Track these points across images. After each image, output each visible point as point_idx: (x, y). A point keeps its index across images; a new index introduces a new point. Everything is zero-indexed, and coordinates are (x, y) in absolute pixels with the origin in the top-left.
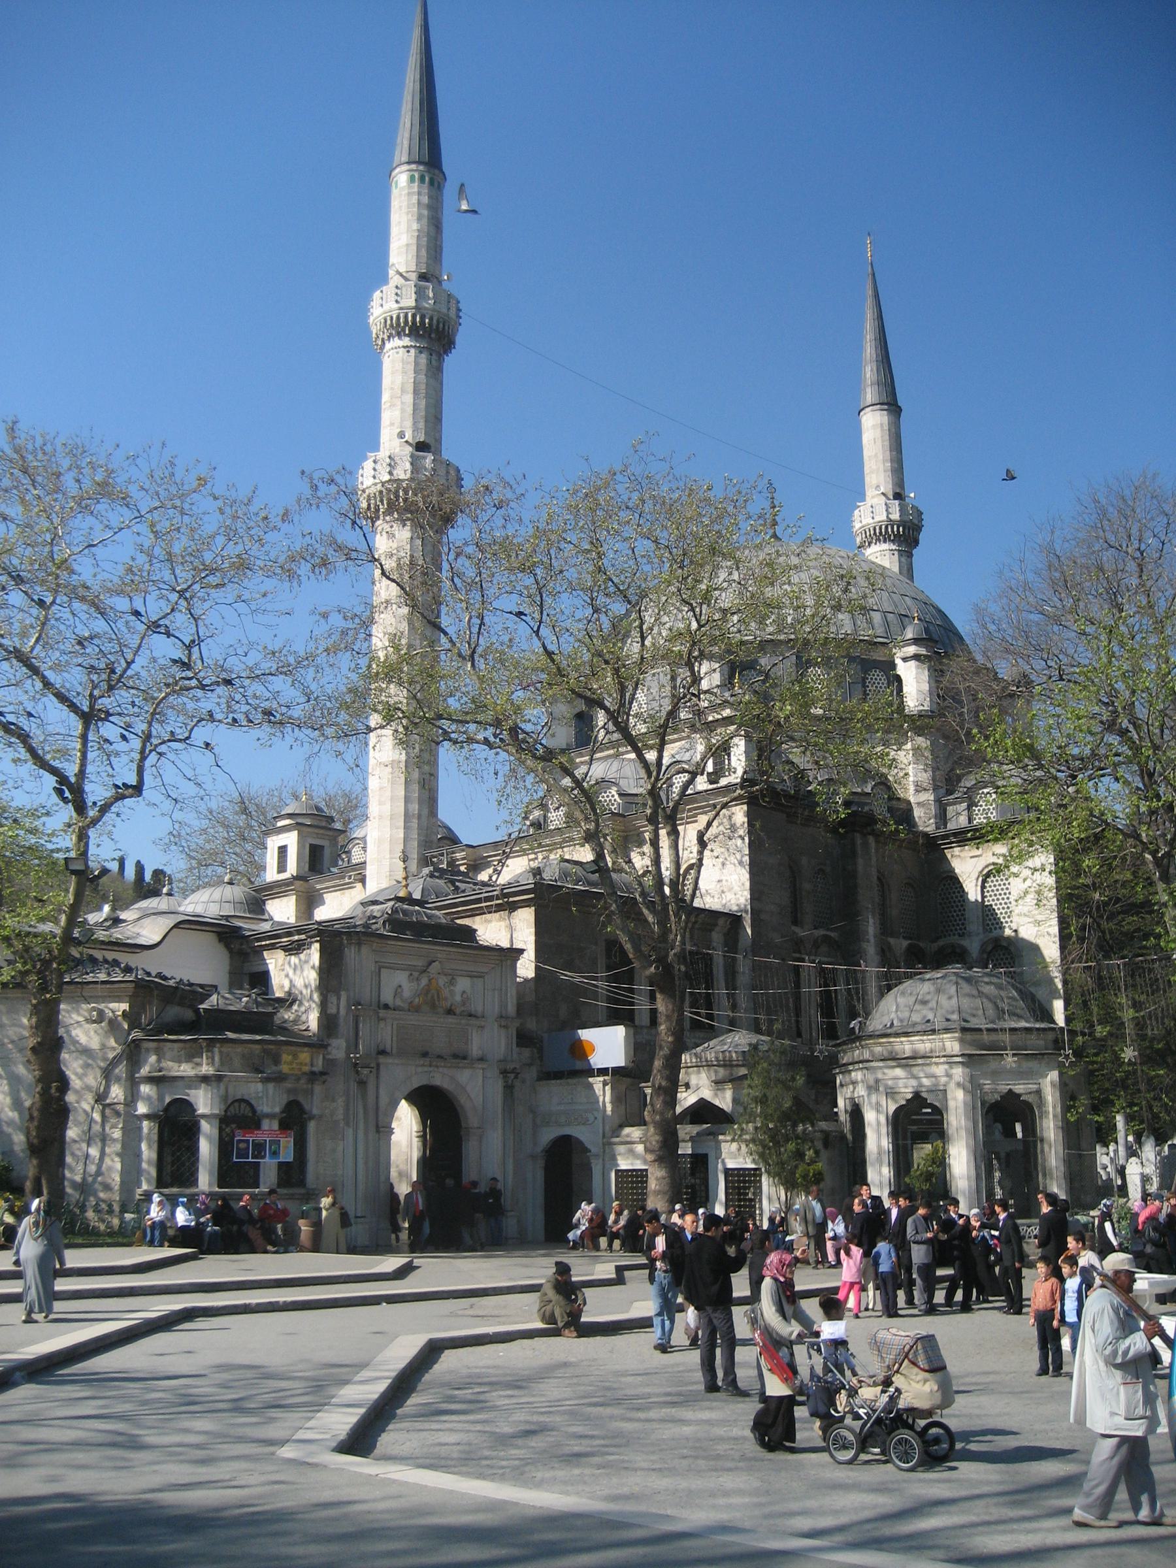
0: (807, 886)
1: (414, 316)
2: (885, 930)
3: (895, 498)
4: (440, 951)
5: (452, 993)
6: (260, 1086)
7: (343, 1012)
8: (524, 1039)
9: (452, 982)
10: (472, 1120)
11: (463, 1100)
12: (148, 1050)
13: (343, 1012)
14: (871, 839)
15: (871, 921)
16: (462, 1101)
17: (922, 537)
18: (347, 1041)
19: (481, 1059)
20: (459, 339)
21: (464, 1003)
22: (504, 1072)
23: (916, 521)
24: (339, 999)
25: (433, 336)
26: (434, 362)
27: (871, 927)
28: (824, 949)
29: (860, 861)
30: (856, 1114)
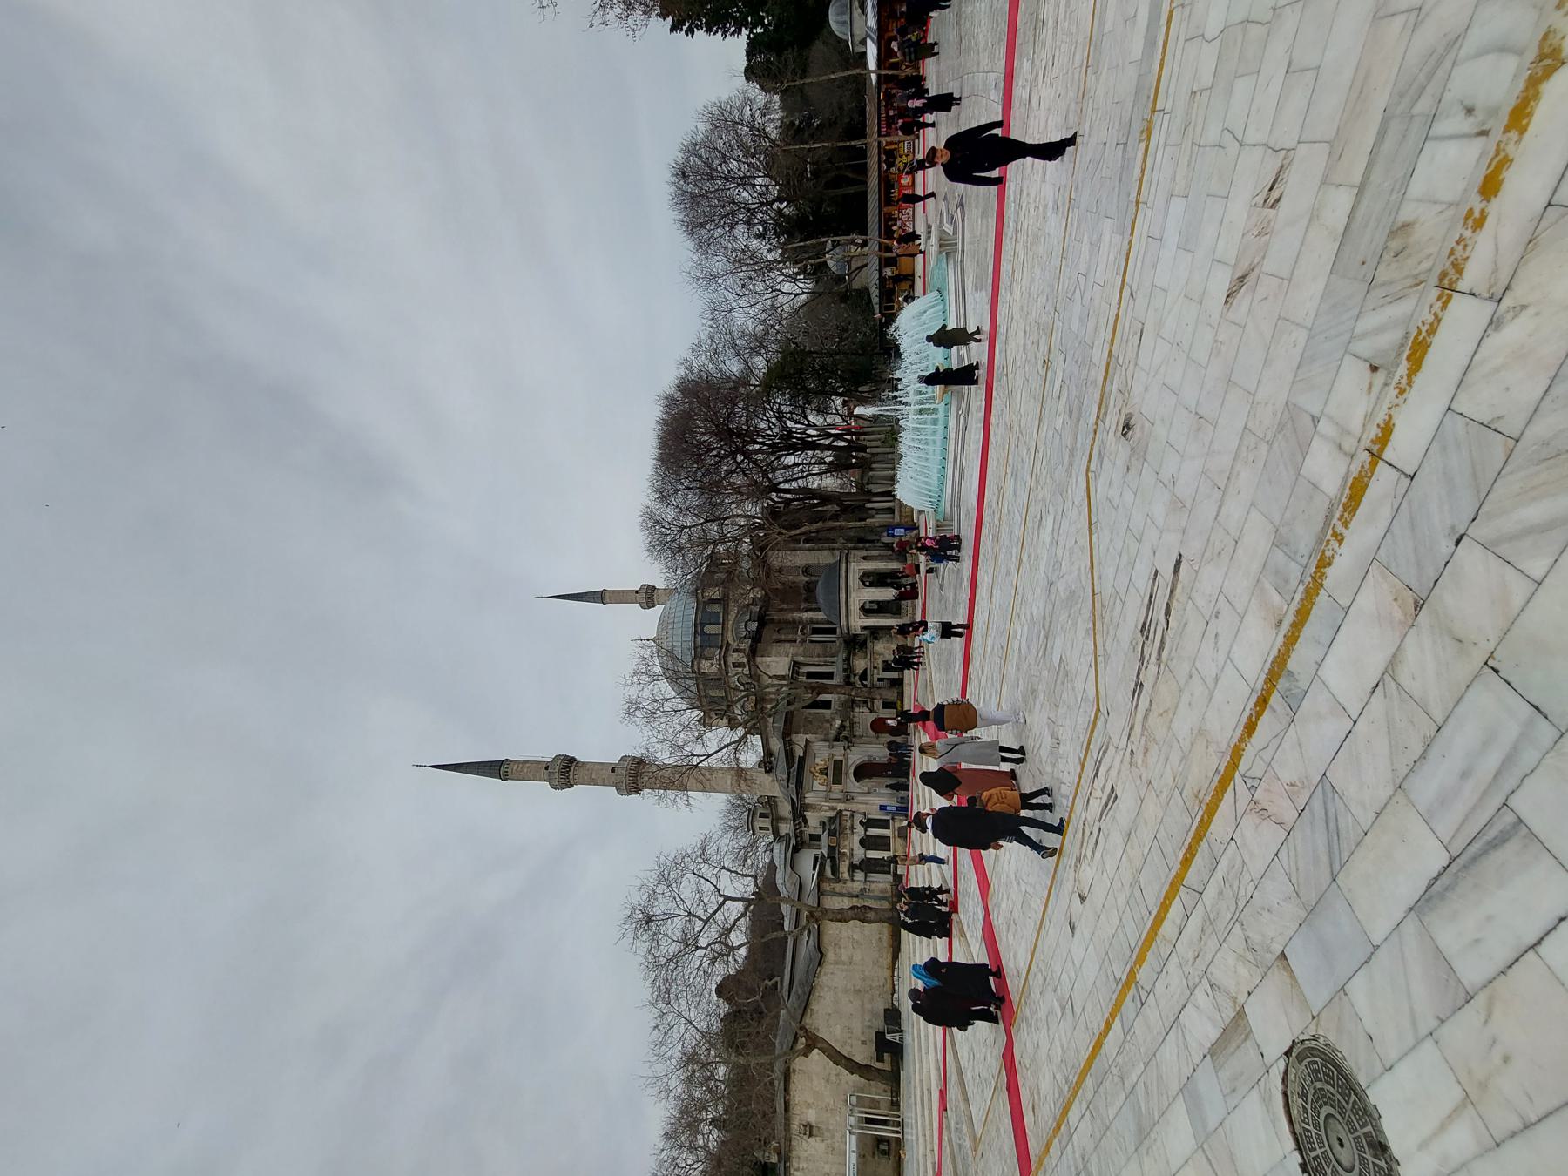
0: (783, 637)
2: (798, 610)
4: (807, 768)
11: (858, 762)
14: (768, 613)
27: (796, 615)
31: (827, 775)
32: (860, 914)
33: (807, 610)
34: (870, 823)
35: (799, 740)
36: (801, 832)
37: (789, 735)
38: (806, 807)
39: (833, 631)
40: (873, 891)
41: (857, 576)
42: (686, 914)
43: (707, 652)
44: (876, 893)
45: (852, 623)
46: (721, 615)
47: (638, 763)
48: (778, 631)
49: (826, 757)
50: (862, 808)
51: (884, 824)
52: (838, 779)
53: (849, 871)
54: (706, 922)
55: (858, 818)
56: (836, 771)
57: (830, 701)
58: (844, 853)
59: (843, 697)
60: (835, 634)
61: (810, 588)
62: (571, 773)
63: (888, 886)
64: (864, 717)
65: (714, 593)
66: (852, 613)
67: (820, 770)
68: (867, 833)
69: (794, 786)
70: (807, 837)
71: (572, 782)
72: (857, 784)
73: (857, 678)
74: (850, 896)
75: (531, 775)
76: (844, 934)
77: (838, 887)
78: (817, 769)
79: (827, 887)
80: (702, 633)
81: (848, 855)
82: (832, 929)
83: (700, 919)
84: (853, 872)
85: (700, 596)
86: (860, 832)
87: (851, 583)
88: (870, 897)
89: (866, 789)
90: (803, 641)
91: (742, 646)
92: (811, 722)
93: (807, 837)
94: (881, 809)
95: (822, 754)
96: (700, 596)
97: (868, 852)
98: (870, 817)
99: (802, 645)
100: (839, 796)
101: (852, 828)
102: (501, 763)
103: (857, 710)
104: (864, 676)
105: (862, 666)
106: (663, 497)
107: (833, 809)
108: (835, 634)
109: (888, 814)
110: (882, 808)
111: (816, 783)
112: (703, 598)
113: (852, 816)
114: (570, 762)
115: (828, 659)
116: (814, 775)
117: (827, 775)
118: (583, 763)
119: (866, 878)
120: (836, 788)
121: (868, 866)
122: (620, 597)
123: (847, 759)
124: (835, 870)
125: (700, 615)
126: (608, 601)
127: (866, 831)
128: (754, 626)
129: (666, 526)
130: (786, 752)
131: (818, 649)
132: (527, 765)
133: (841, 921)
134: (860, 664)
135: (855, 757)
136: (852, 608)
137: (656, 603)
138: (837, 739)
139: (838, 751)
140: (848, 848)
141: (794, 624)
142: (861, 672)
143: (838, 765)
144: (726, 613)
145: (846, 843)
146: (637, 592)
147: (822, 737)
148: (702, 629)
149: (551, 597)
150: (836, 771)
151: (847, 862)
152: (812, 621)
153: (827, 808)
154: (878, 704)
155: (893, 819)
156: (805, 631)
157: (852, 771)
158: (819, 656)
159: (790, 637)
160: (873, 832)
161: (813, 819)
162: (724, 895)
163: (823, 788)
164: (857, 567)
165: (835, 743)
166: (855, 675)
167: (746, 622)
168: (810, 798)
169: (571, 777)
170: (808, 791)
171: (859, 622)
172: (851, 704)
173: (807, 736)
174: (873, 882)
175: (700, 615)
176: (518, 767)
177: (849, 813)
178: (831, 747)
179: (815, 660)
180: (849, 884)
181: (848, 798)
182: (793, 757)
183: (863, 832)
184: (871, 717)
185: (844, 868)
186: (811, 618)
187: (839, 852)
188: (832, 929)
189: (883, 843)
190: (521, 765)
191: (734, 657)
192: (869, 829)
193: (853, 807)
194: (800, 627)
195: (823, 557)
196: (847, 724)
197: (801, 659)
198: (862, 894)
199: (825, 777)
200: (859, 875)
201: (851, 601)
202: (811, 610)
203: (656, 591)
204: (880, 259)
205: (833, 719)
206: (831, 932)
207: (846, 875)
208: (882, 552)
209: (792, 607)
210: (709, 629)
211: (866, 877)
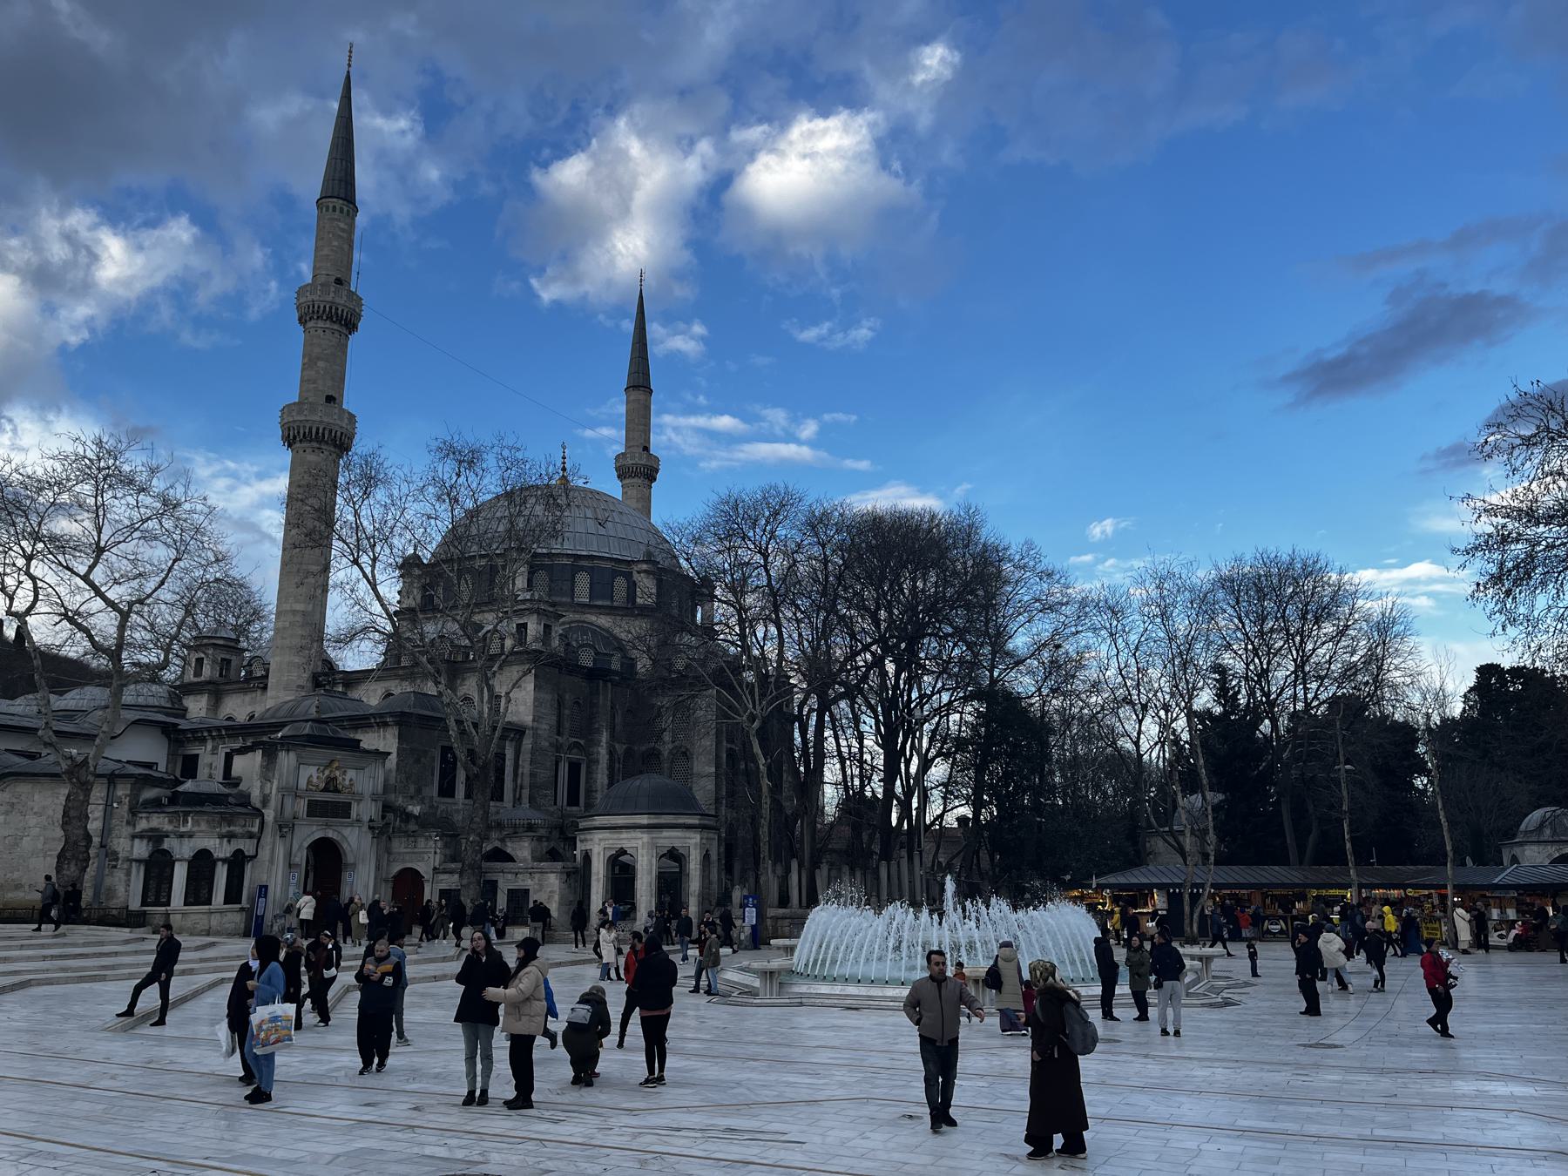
0: (567, 712)
1: (331, 308)
4: (339, 755)
5: (344, 779)
6: (218, 840)
7: (274, 792)
9: (344, 773)
11: (345, 846)
13: (274, 792)
14: (609, 685)
18: (275, 811)
24: (272, 784)
27: (604, 737)
29: (601, 697)
30: (587, 858)
31: (325, 790)
32: (75, 849)
33: (611, 753)
34: (238, 863)
35: (384, 740)
36: (203, 741)
37: (398, 723)
38: (270, 752)
39: (573, 799)
40: (111, 874)
41: (677, 844)
42: (102, 544)
43: (542, 576)
44: (108, 881)
45: (598, 835)
46: (608, 603)
48: (577, 703)
49: (358, 788)
50: (265, 854)
51: (233, 895)
52: (316, 809)
53: (152, 830)
54: (85, 578)
55: (247, 846)
56: (330, 807)
57: (453, 796)
59: (458, 818)
60: (569, 805)
61: (651, 760)
62: (328, 324)
63: (116, 903)
64: (426, 857)
65: (647, 588)
66: (616, 836)
67: (336, 778)
68: (220, 863)
69: (306, 731)
70: (194, 750)
71: (310, 324)
72: (306, 845)
73: (497, 844)
74: (106, 831)
75: (326, 251)
76: (32, 820)
77: (124, 811)
78: (337, 773)
79: (122, 791)
80: (576, 569)
81: (182, 829)
82: (49, 801)
83: (91, 568)
84: (150, 839)
85: (645, 567)
86: (222, 850)
87: (666, 833)
88: (100, 869)
89: (297, 860)
91: (556, 643)
92: (418, 761)
93: (194, 750)
94: (261, 887)
95: (363, 782)
96: (645, 567)
97: (185, 865)
98: (248, 868)
100: (288, 812)
101: (230, 836)
104: (501, 856)
105: (519, 853)
106: (816, 523)
107: (265, 800)
108: (569, 805)
109: (252, 900)
110: (263, 890)
111: (313, 770)
112: (638, 572)
113: (251, 836)
114: (348, 323)
115: (526, 793)
116: (327, 767)
117: (325, 790)
119: (136, 861)
120: (302, 806)
121: (158, 868)
122: (639, 424)
123: (351, 825)
124: (155, 805)
125: (608, 565)
126: (632, 398)
127: (224, 860)
128: (586, 660)
129: (768, 528)
130: (366, 717)
131: (544, 775)
132: (346, 247)
133: (65, 814)
134: (522, 850)
135: (355, 840)
136: (625, 835)
137: (627, 481)
138: (387, 808)
139: (366, 810)
140: (195, 829)
141: (587, 731)
142: (509, 850)
143: (341, 811)
144: (611, 610)
145: (204, 826)
146: (646, 449)
147: (392, 781)
148: (582, 569)
150: (330, 807)
151: (168, 827)
152: (592, 762)
153: (267, 791)
154: (450, 881)
155: (242, 909)
156: (575, 751)
157: (330, 834)
158: (532, 775)
159: (567, 725)
160: (221, 874)
161: (247, 765)
162: (130, 610)
163: (303, 784)
164: (692, 844)
165: (380, 804)
166: (502, 840)
167: (593, 647)
168: (286, 760)
169: (321, 324)
170: (299, 756)
171: (598, 846)
172: (450, 834)
173: (393, 758)
174: (128, 874)
175: (608, 565)
176: (343, 230)
177: (255, 829)
178: (374, 797)
179: (525, 768)
180: (129, 830)
181: (285, 827)
182: (356, 728)
183: (221, 855)
184: (424, 868)
185: (158, 821)
186: (597, 762)
187: (186, 814)
188: (49, 801)
189: (198, 892)
190: (345, 235)
191: (534, 627)
192: (226, 866)
193: (267, 838)
194: (582, 742)
195: (704, 789)
196: (412, 827)
197: (527, 743)
198: (106, 856)
199: (322, 786)
200: (141, 849)
201: (637, 834)
203: (646, 482)
204: (1179, 885)
205: (422, 802)
206: (36, 797)
207: (143, 825)
208: (715, 886)
209: (618, 728)
210: (583, 582)
211: (139, 861)
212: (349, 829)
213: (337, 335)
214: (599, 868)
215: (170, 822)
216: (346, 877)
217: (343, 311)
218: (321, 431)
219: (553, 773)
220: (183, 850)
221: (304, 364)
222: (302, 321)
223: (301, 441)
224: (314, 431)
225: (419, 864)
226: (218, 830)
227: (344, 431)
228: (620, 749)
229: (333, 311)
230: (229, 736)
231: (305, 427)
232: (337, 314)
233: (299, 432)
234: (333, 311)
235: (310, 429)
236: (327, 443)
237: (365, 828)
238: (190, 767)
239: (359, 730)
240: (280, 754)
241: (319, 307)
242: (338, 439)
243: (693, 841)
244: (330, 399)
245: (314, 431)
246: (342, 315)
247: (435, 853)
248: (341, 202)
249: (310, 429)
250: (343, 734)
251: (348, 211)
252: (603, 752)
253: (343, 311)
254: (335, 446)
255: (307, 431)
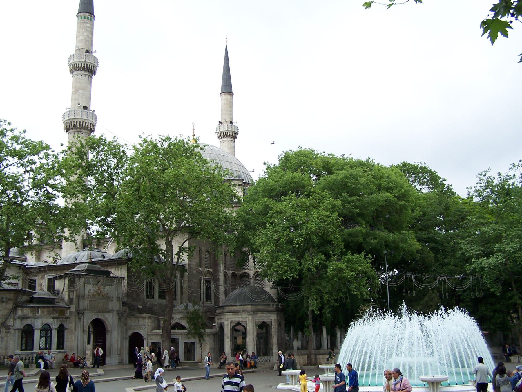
0: (203, 256)
1: (84, 64)
2: (225, 268)
3: (230, 123)
5: (104, 291)
6: (52, 320)
7: (74, 297)
8: (124, 304)
10: (109, 328)
12: (19, 310)
13: (74, 297)
15: (222, 266)
16: (106, 323)
17: (238, 136)
19: (112, 310)
20: (98, 71)
21: (107, 293)
22: (118, 314)
23: (236, 131)
24: (73, 293)
25: (90, 71)
26: (90, 80)
27: (222, 268)
28: (208, 274)
30: (221, 327)
34: (61, 330)
35: (121, 272)
41: (266, 320)
47: (91, 129)
48: (208, 251)
58: (38, 312)
62: (83, 72)
71: (75, 73)
72: (90, 321)
90: (200, 273)
97: (39, 331)
99: (197, 272)
102: (92, 14)
103: (150, 321)
118: (91, 82)
132: (90, 36)
137: (222, 139)
149: (226, 49)
152: (217, 280)
153: (71, 297)
157: (100, 317)
159: (204, 262)
164: (272, 318)
165: (121, 302)
169: (79, 72)
176: (89, 27)
179: (185, 285)
182: (107, 266)
194: (211, 270)
202: (225, 279)
209: (228, 263)
211: (18, 329)
212: (108, 314)
213: (87, 77)
214: (228, 331)
215: (31, 312)
216: (108, 337)
217: (90, 65)
218: (81, 123)
219: (199, 286)
220: (38, 324)
221: (73, 92)
222: (72, 71)
223: (72, 129)
224: (78, 124)
225: (141, 330)
226: (52, 315)
227: (92, 123)
228: (230, 272)
229: (85, 66)
230: (49, 270)
231: (74, 122)
232: (87, 67)
233: (71, 125)
234: (85, 66)
235: (77, 122)
236: (84, 129)
237: (115, 313)
238: (32, 285)
239: (109, 267)
240: (76, 279)
241: (79, 64)
242: (89, 127)
243: (274, 318)
244: (85, 108)
245: (78, 124)
246: (89, 68)
247: (148, 325)
248: (88, 14)
249: (77, 122)
250: (103, 269)
251: (91, 19)
252: (221, 275)
253: (90, 65)
254: (88, 130)
255: (75, 123)
